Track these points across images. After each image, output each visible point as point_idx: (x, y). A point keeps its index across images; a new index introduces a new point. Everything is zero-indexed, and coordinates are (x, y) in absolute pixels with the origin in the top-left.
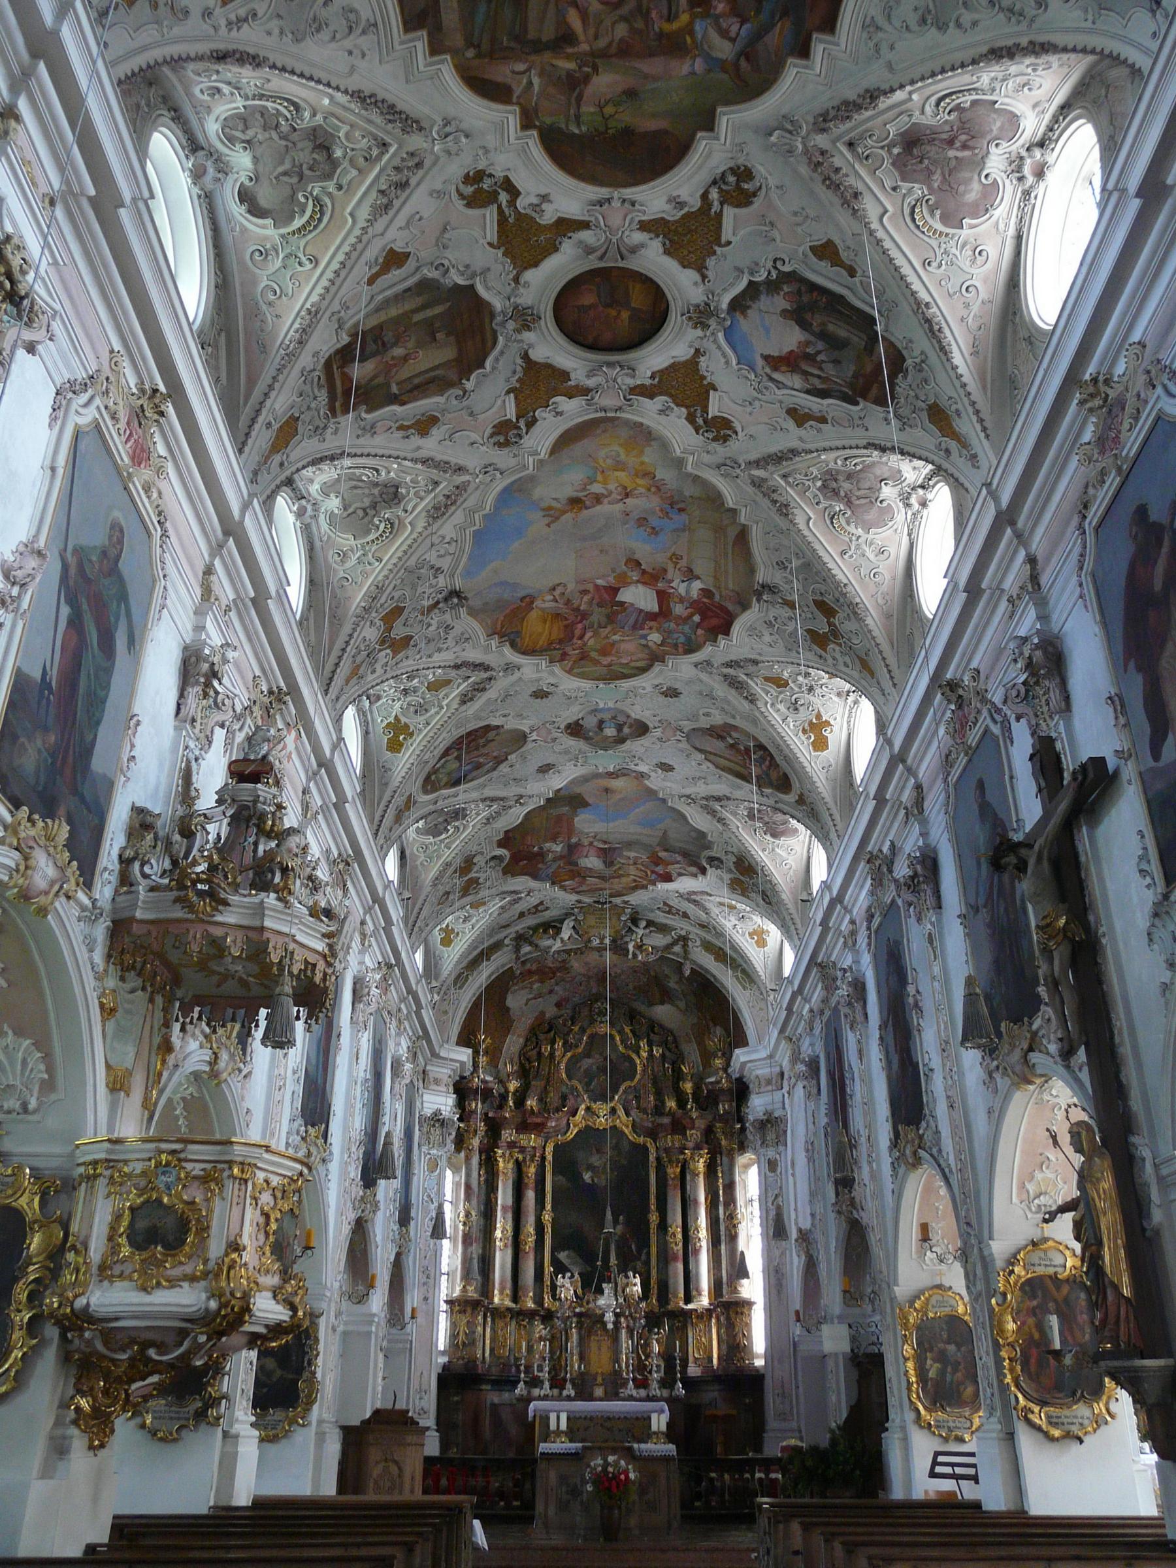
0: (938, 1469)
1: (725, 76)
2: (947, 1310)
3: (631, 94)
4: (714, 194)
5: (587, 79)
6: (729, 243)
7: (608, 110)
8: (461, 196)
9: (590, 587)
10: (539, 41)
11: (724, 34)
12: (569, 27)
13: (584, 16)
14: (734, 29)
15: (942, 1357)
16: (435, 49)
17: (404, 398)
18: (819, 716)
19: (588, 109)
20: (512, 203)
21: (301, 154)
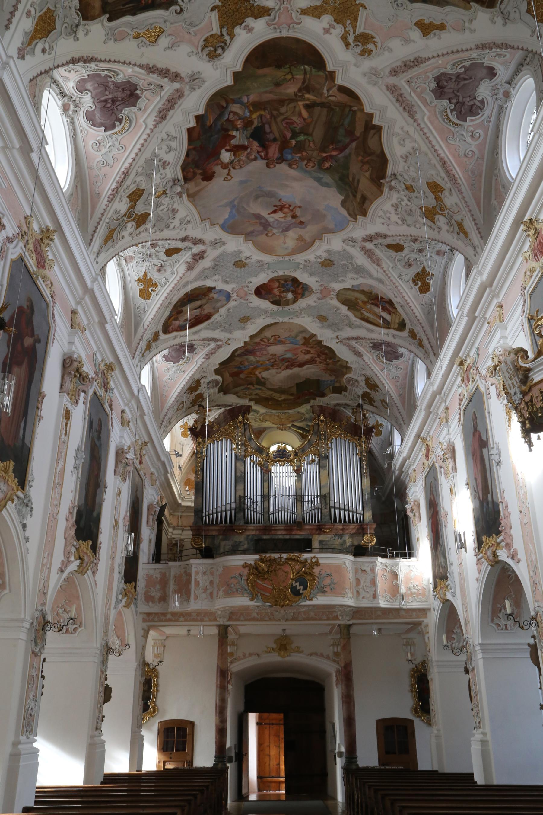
1: (232, 97)
3: (277, 84)
4: (227, 38)
5: (300, 90)
6: (212, 10)
7: (289, 77)
8: (374, 43)
10: (322, 107)
11: (235, 113)
12: (308, 111)
13: (300, 115)
14: (231, 116)
16: (371, 116)
19: (300, 77)
20: (347, 33)
21: (452, 86)
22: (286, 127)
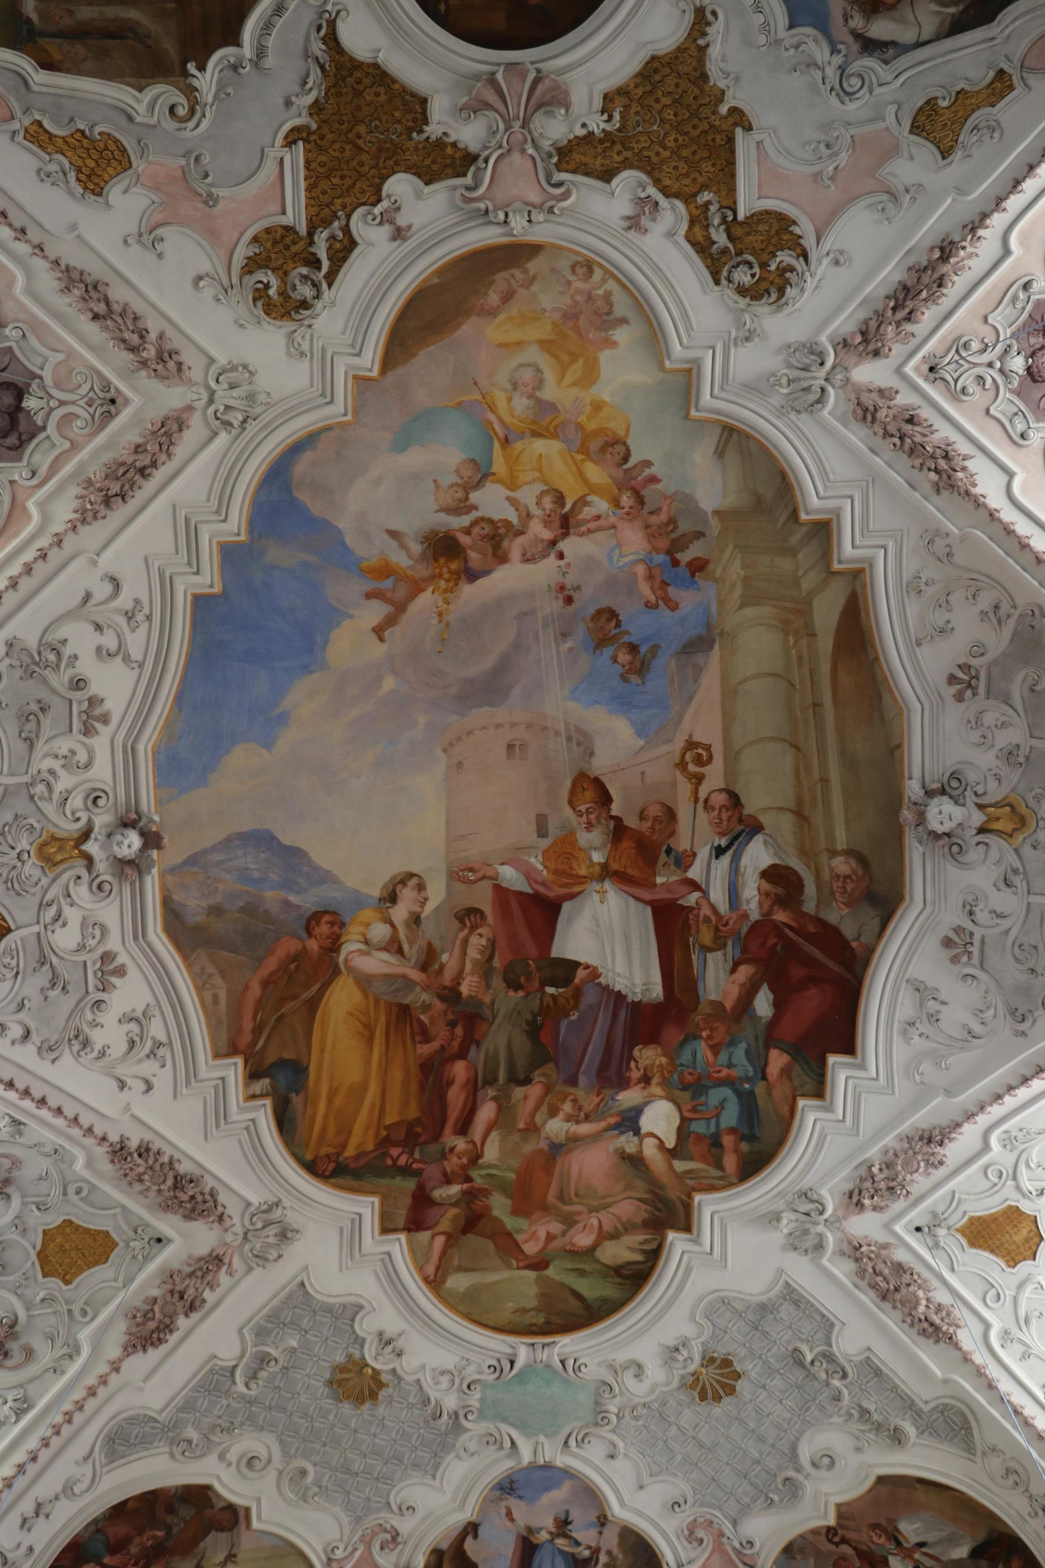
9: (483, 898)
17: (54, 48)
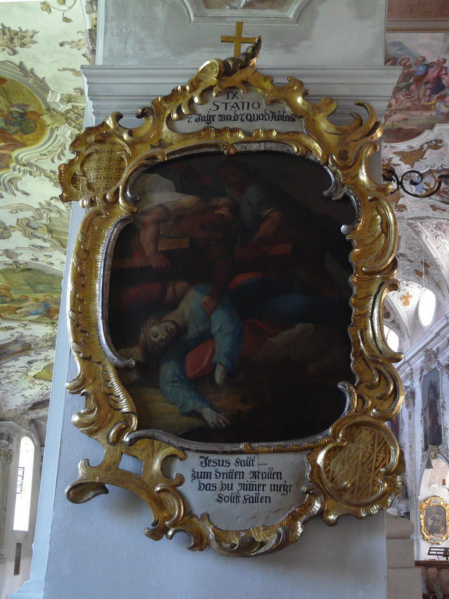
0: (431, 553)
1: (443, 117)
2: (437, 504)
15: (434, 519)
18: (408, 294)
22: (412, 92)
